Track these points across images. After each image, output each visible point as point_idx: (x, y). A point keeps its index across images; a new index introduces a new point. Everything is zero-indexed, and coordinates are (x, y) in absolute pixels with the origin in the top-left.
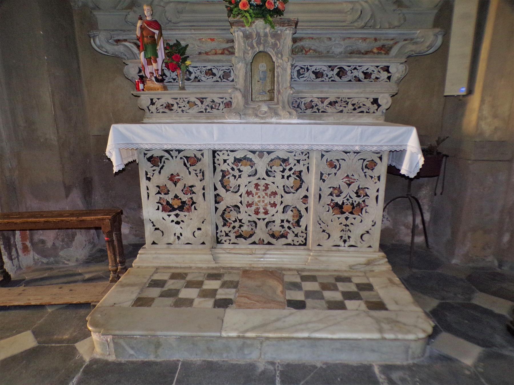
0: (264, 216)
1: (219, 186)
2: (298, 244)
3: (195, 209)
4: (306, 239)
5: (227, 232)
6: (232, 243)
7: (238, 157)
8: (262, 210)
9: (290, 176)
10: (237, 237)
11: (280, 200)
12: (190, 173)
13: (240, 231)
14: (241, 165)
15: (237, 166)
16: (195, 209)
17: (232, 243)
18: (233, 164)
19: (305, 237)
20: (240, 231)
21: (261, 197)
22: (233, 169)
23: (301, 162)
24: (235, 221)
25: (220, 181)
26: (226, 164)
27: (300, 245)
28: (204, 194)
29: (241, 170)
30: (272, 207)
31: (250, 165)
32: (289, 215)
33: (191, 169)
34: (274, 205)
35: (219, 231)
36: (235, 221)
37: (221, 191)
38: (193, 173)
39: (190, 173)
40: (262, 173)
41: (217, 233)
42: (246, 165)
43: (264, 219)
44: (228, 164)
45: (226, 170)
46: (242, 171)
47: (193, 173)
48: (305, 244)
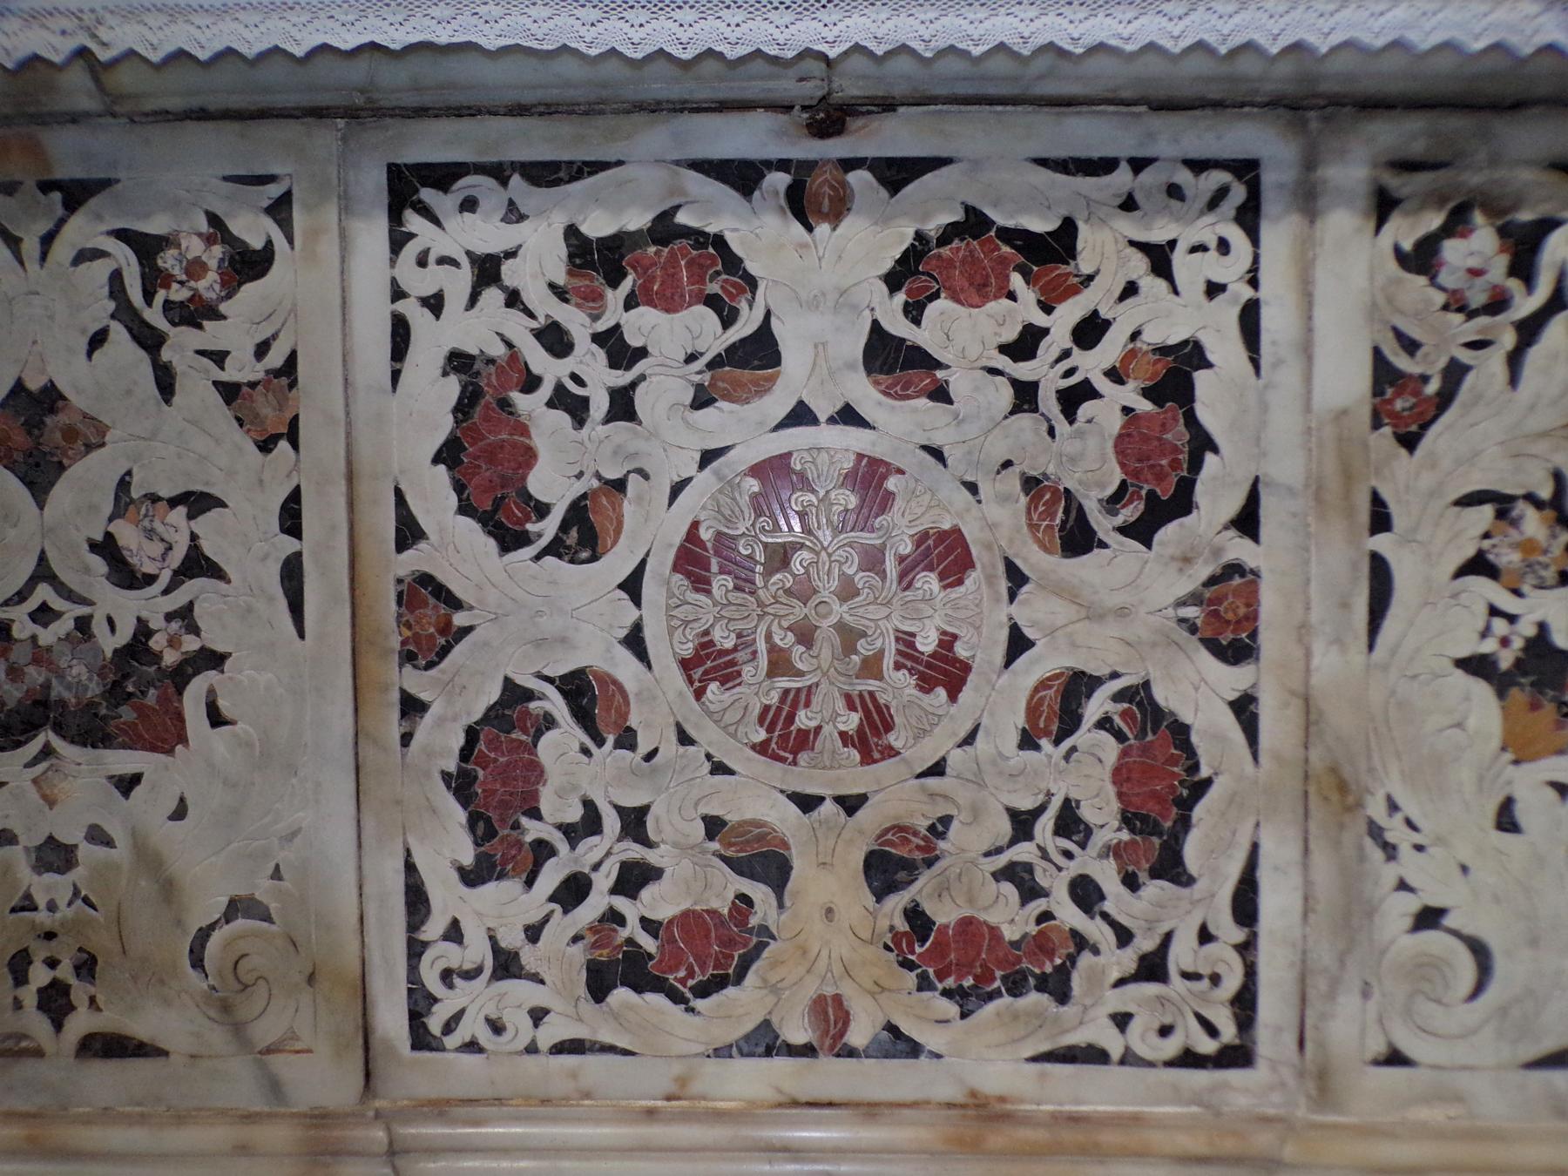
0: (856, 778)
1: (435, 498)
2: (1171, 1047)
3: (216, 718)
4: (1245, 1004)
5: (512, 938)
6: (560, 1049)
7: (597, 226)
8: (831, 716)
9: (1086, 391)
10: (599, 984)
11: (998, 618)
12: (166, 383)
13: (633, 929)
14: (630, 303)
15: (592, 301)
16: (216, 718)
17: (560, 1049)
18: (560, 293)
19: (1233, 981)
20: (633, 929)
21: (828, 587)
22: (555, 340)
23: (1179, 259)
24: (573, 833)
25: (448, 454)
26: (492, 297)
27: (1189, 1059)
28: (292, 573)
29: (634, 341)
30: (926, 685)
31: (712, 302)
32: (1088, 772)
33: (181, 345)
34: (945, 671)
35: (433, 929)
36: (573, 833)
37: (458, 548)
38: (196, 385)
39: (166, 383)
40: (819, 352)
41: (416, 949)
42: (670, 303)
43: (851, 804)
44: (513, 299)
45: (498, 350)
46: (642, 353)
47: (196, 385)
48: (1237, 1056)
